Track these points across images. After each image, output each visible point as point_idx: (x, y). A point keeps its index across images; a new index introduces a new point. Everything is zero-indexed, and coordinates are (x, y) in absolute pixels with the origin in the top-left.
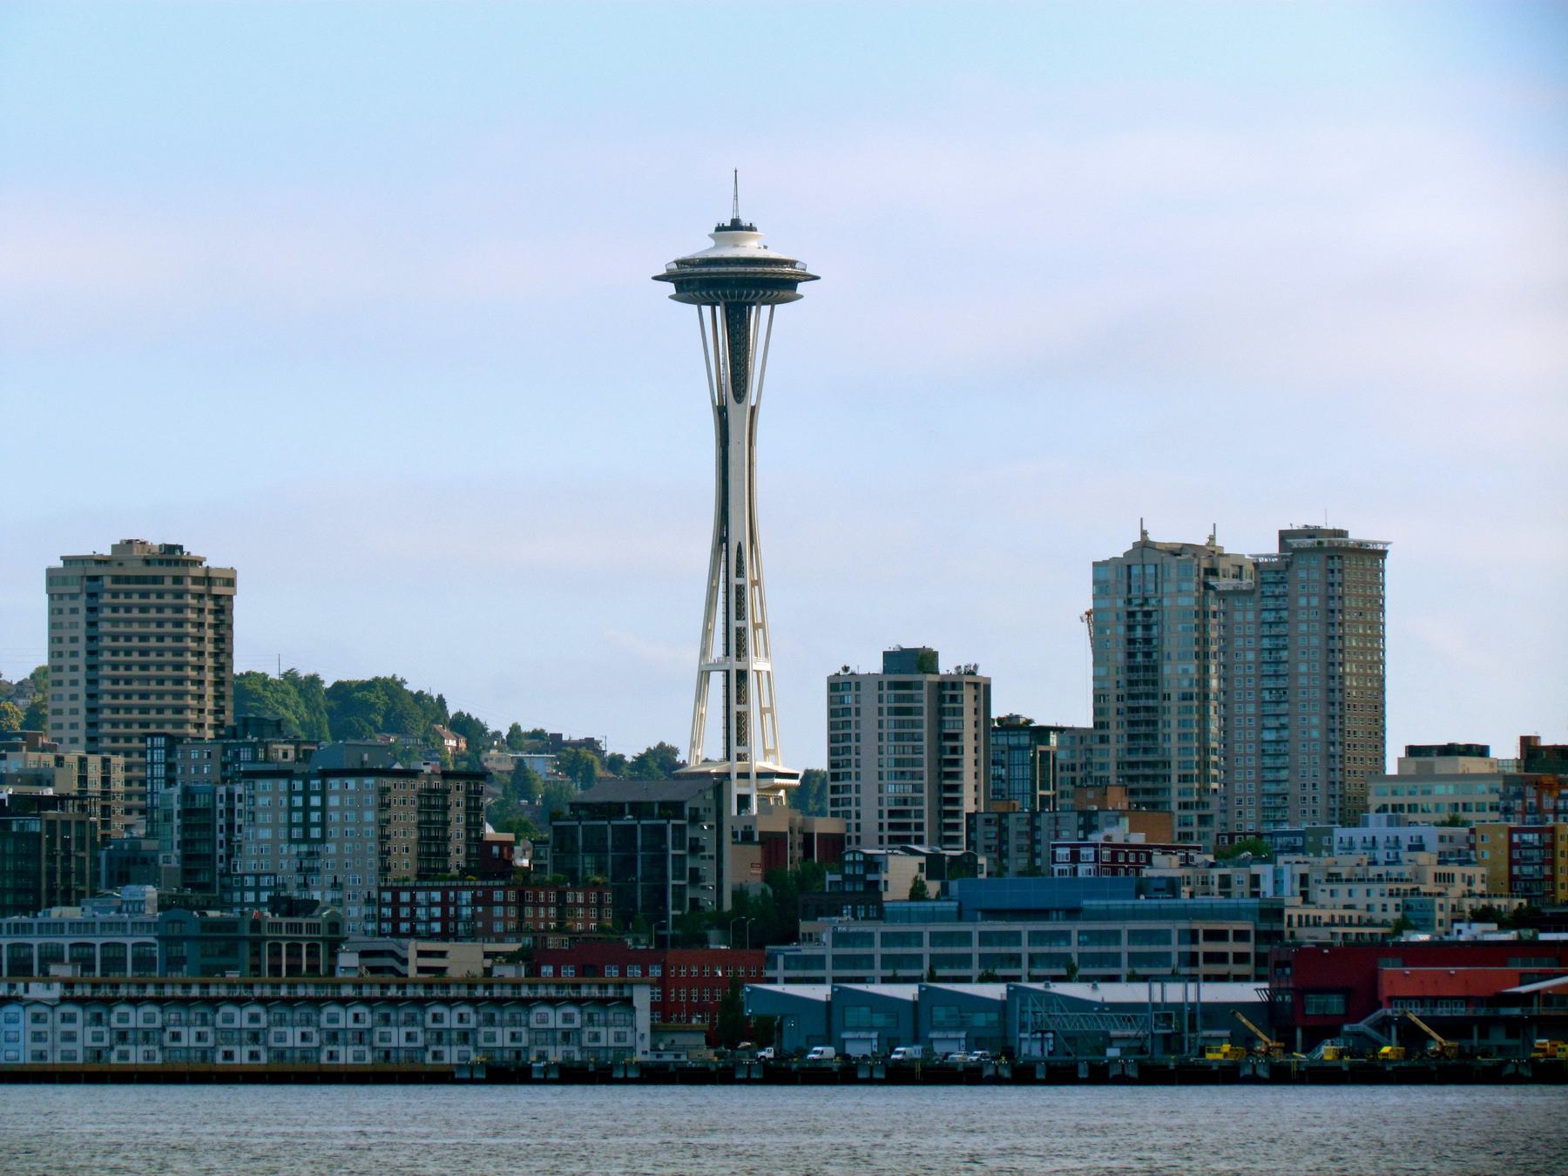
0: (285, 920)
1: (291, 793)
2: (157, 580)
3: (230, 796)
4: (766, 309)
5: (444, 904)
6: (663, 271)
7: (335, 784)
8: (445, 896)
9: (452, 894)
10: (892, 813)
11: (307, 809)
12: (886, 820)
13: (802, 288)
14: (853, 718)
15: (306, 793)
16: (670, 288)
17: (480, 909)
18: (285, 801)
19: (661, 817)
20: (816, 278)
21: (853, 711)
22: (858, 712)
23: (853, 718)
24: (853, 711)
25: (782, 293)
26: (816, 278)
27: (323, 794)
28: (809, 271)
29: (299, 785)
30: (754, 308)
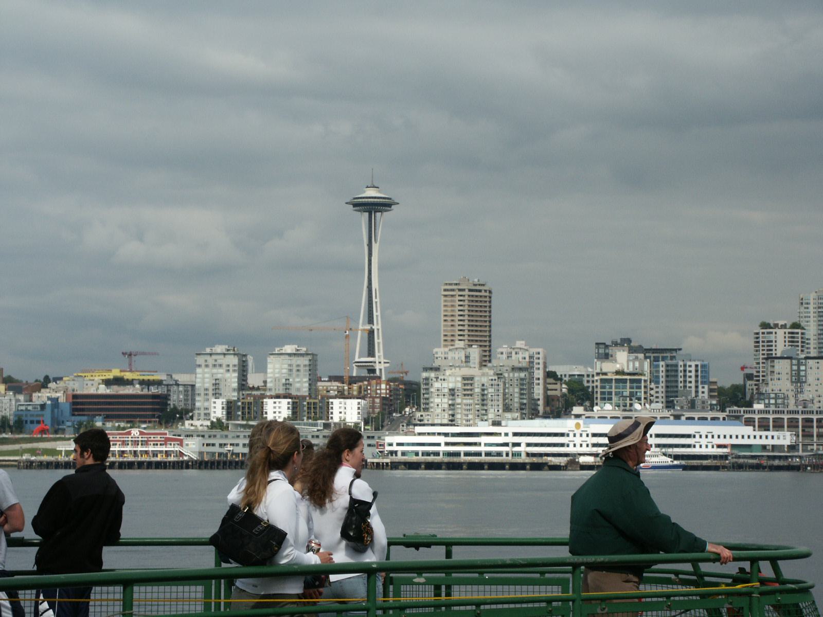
1: (792, 365)
2: (480, 291)
3: (685, 366)
4: (378, 214)
6: (348, 201)
7: (808, 361)
11: (799, 370)
13: (393, 207)
14: (774, 344)
15: (799, 365)
16: (352, 206)
18: (789, 367)
20: (398, 204)
21: (774, 342)
22: (776, 341)
23: (774, 344)
24: (774, 342)
25: (386, 208)
26: (398, 204)
27: (805, 365)
28: (396, 201)
29: (794, 362)
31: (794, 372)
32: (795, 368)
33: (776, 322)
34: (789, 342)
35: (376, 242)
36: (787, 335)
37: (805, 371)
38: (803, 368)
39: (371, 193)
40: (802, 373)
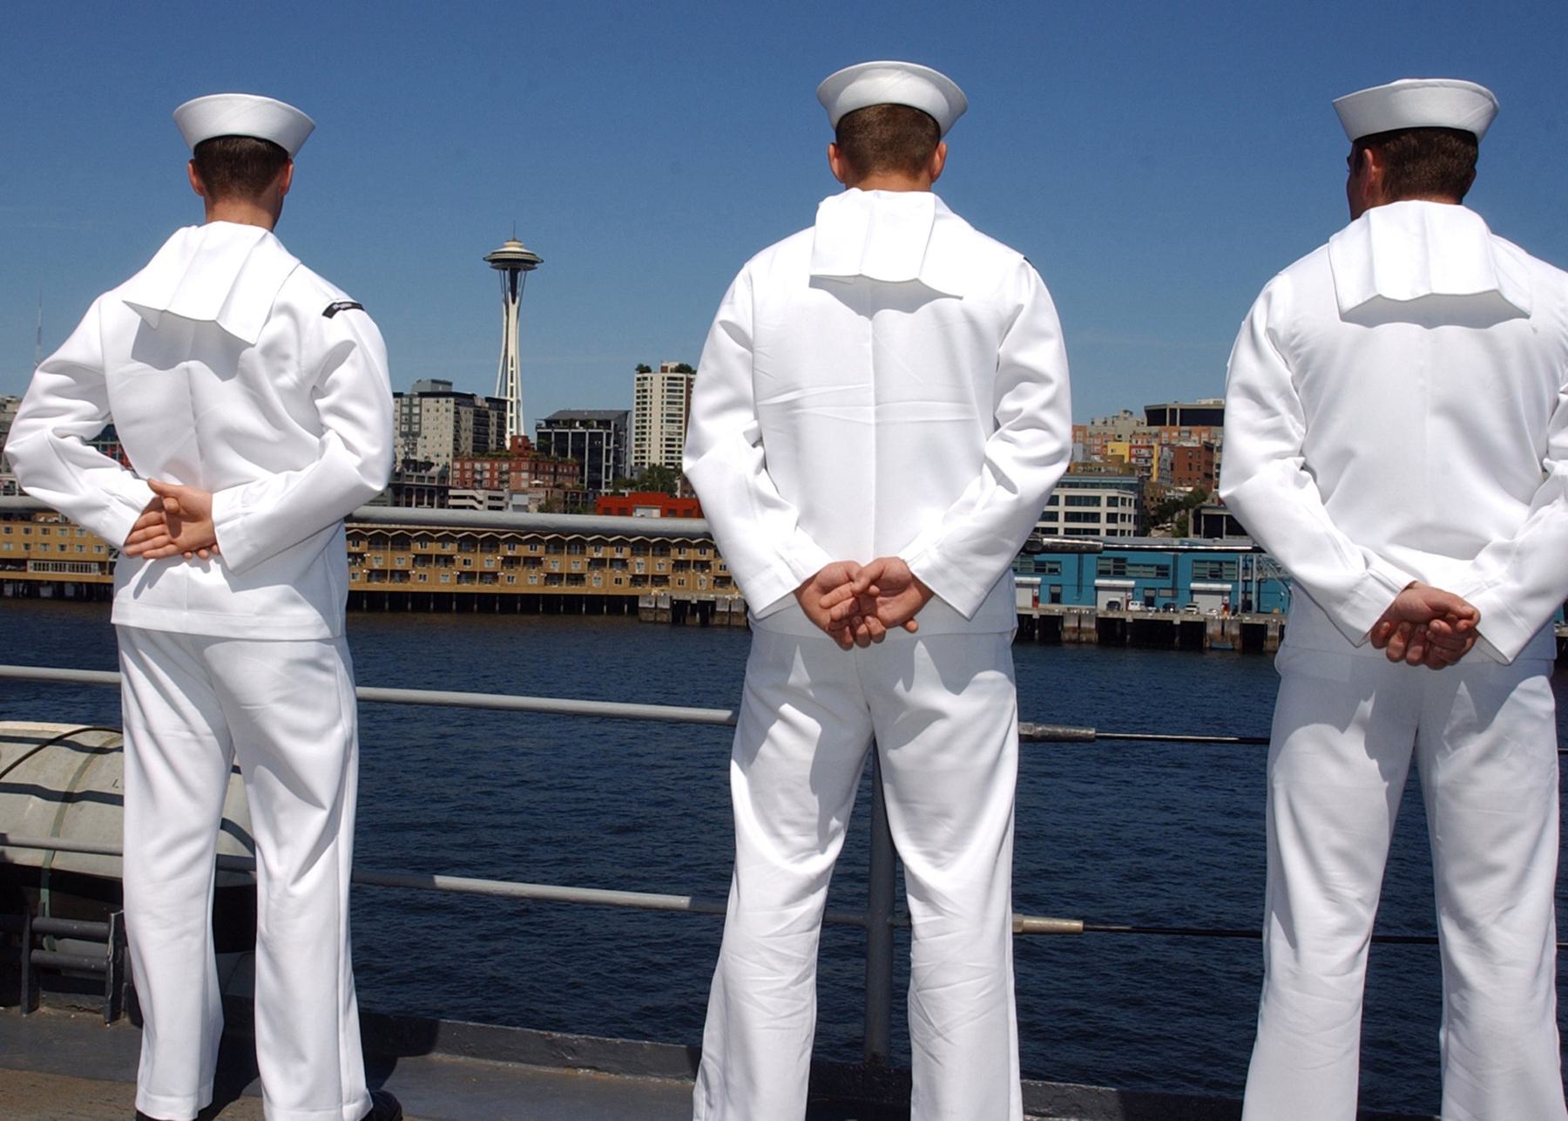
0: (415, 474)
1: (402, 406)
5: (492, 470)
8: (492, 466)
9: (496, 465)
10: (667, 439)
11: (411, 414)
12: (664, 442)
13: (537, 265)
14: (648, 394)
16: (490, 264)
17: (513, 474)
19: (598, 428)
23: (648, 394)
27: (420, 405)
30: (519, 274)
31: (404, 417)
32: (406, 410)
33: (664, 365)
34: (669, 391)
35: (514, 302)
36: (666, 382)
37: (420, 414)
38: (416, 410)
39: (513, 248)
40: (415, 419)
